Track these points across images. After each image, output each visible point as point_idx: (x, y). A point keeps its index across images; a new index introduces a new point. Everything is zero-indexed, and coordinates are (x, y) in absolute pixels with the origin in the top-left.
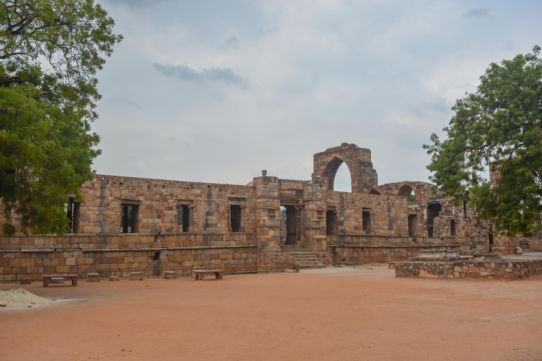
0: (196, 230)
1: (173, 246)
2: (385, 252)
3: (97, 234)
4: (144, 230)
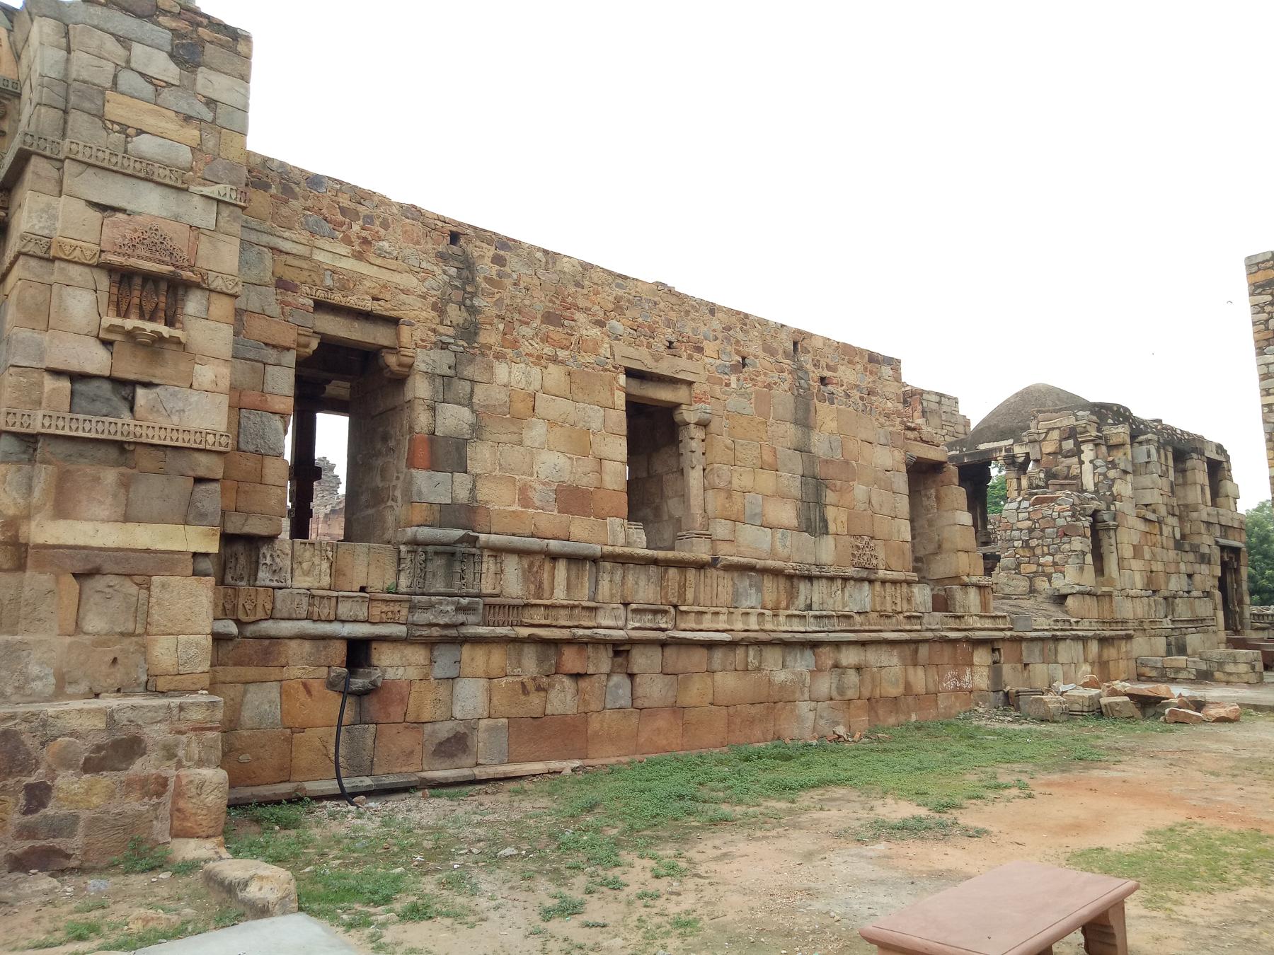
2: (780, 676)
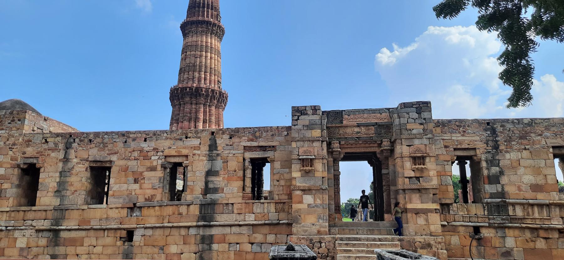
1: (152, 222)
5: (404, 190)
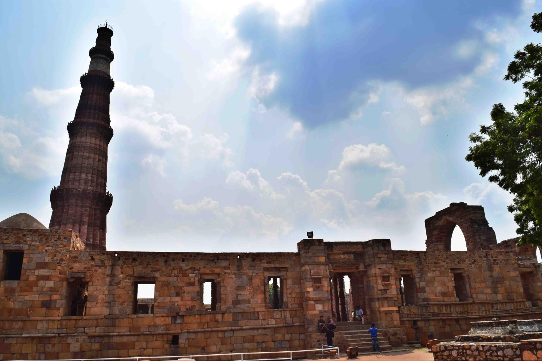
0: (223, 308)
1: (194, 327)
3: (105, 316)
4: (159, 310)
5: (378, 299)
